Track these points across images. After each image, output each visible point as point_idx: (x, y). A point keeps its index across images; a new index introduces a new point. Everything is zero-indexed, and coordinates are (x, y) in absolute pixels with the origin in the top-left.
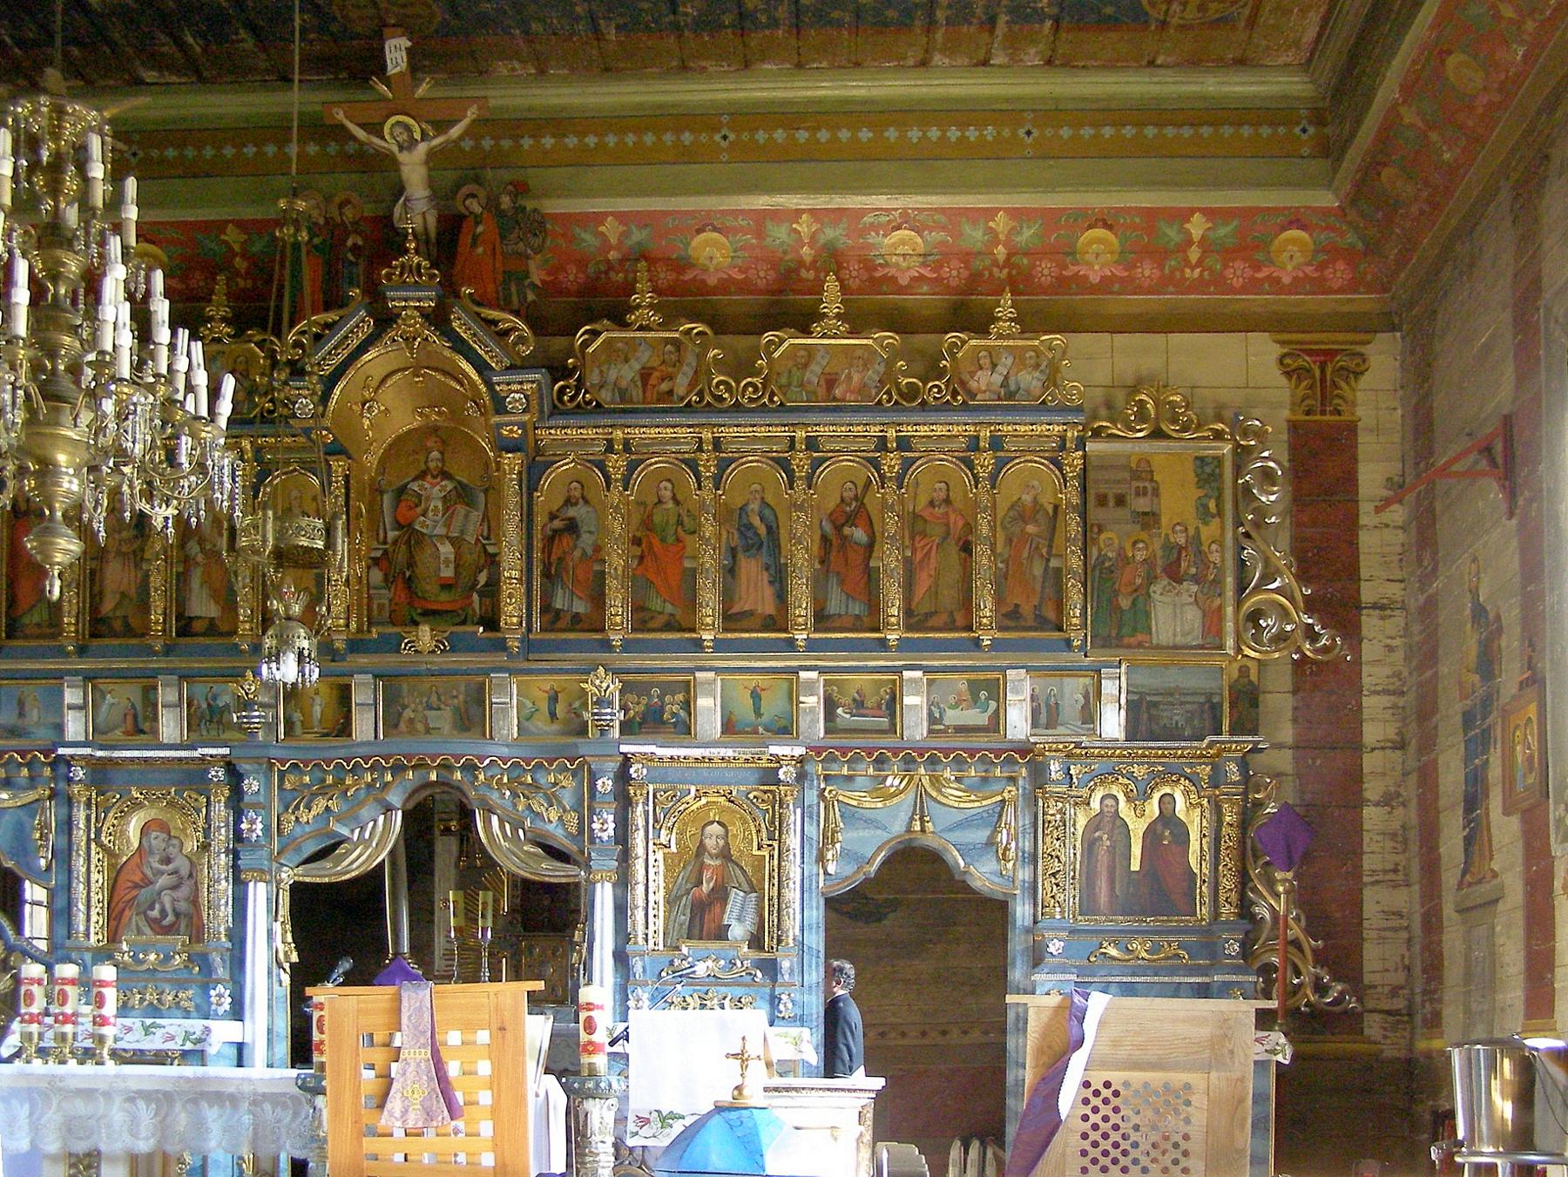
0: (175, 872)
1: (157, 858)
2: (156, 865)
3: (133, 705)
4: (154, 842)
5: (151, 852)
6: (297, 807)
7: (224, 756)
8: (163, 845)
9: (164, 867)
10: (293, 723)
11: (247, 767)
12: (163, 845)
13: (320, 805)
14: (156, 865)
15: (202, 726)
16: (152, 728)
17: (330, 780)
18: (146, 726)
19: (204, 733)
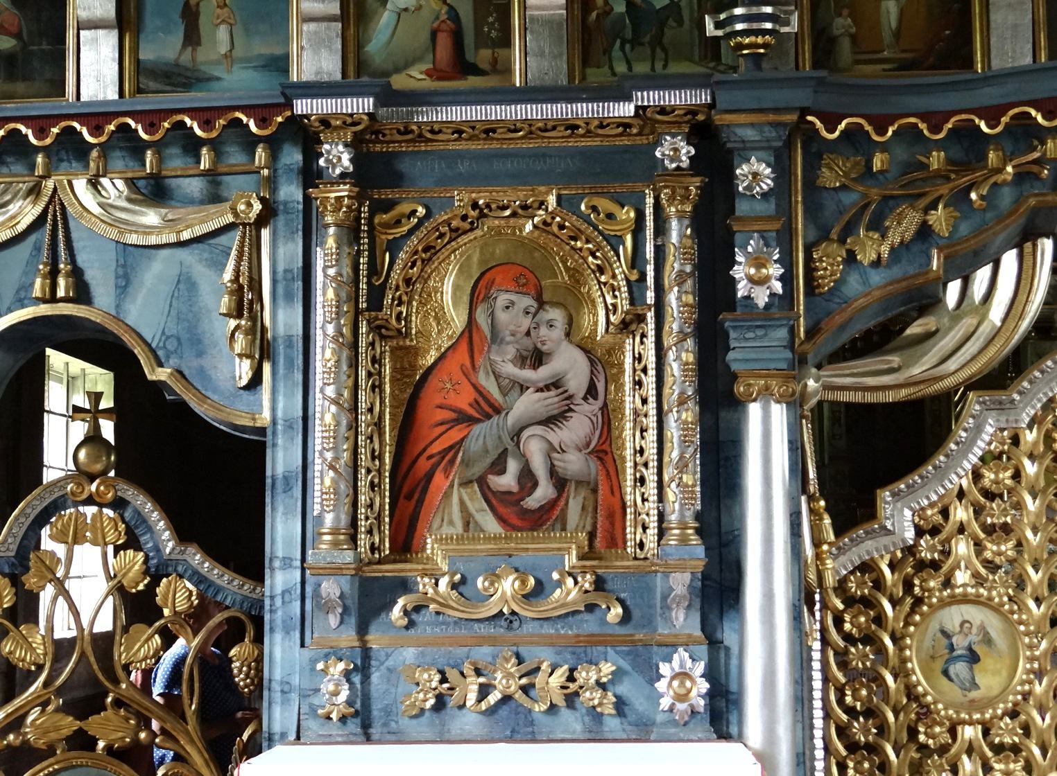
0: (555, 384)
1: (511, 351)
2: (510, 369)
3: (454, 15)
4: (502, 316)
5: (496, 337)
6: (849, 229)
7: (692, 111)
8: (526, 322)
9: (527, 374)
10: (833, 40)
11: (750, 134)
12: (526, 322)
13: (903, 227)
14: (510, 369)
15: (616, 52)
16: (495, 62)
17: (936, 160)
18: (483, 57)
19: (621, 68)
